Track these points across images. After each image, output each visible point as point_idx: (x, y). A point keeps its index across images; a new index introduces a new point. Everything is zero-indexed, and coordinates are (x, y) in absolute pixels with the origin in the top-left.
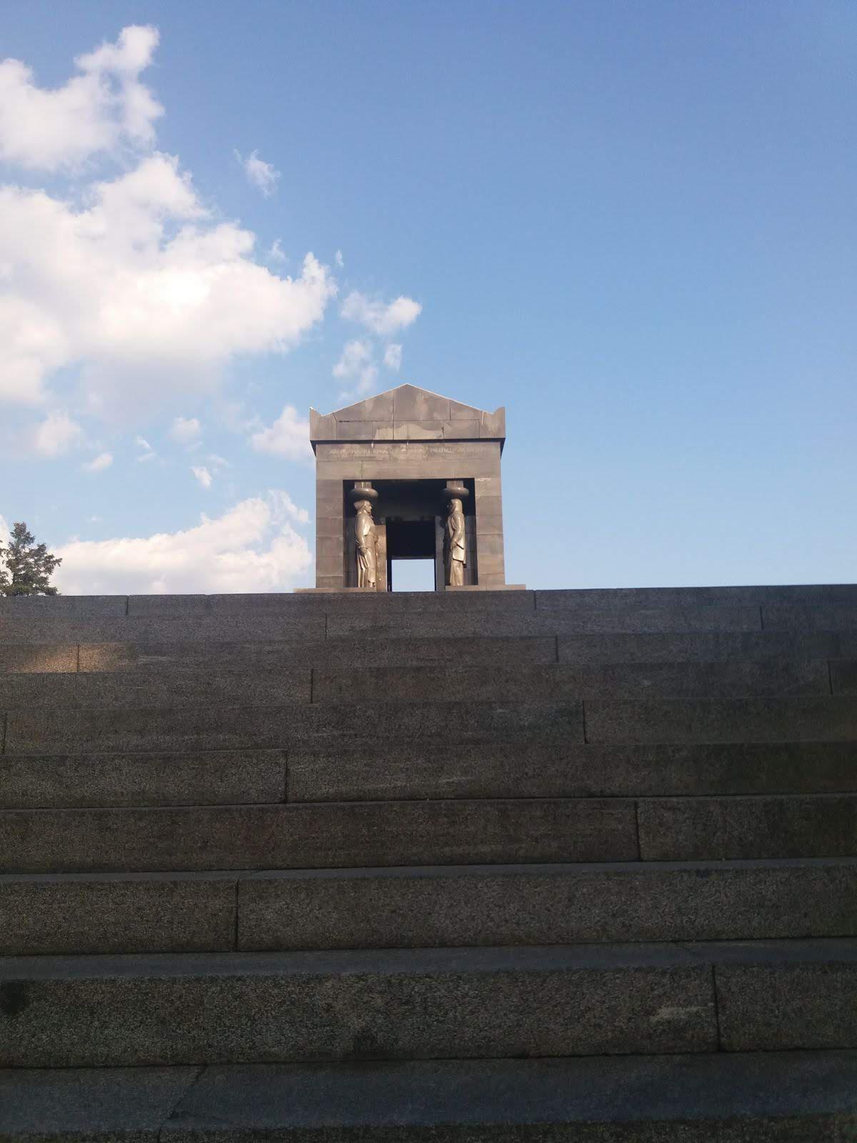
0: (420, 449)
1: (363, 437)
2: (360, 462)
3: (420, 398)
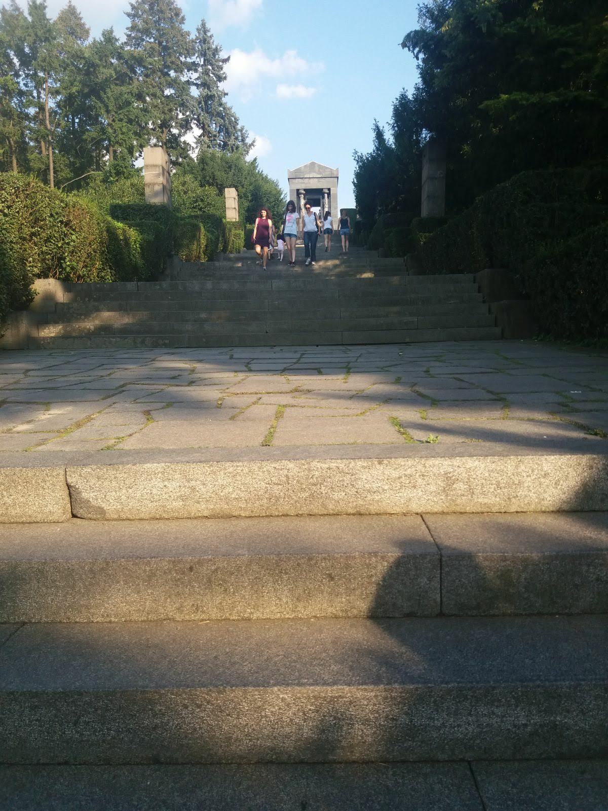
1: (302, 177)
3: (316, 165)
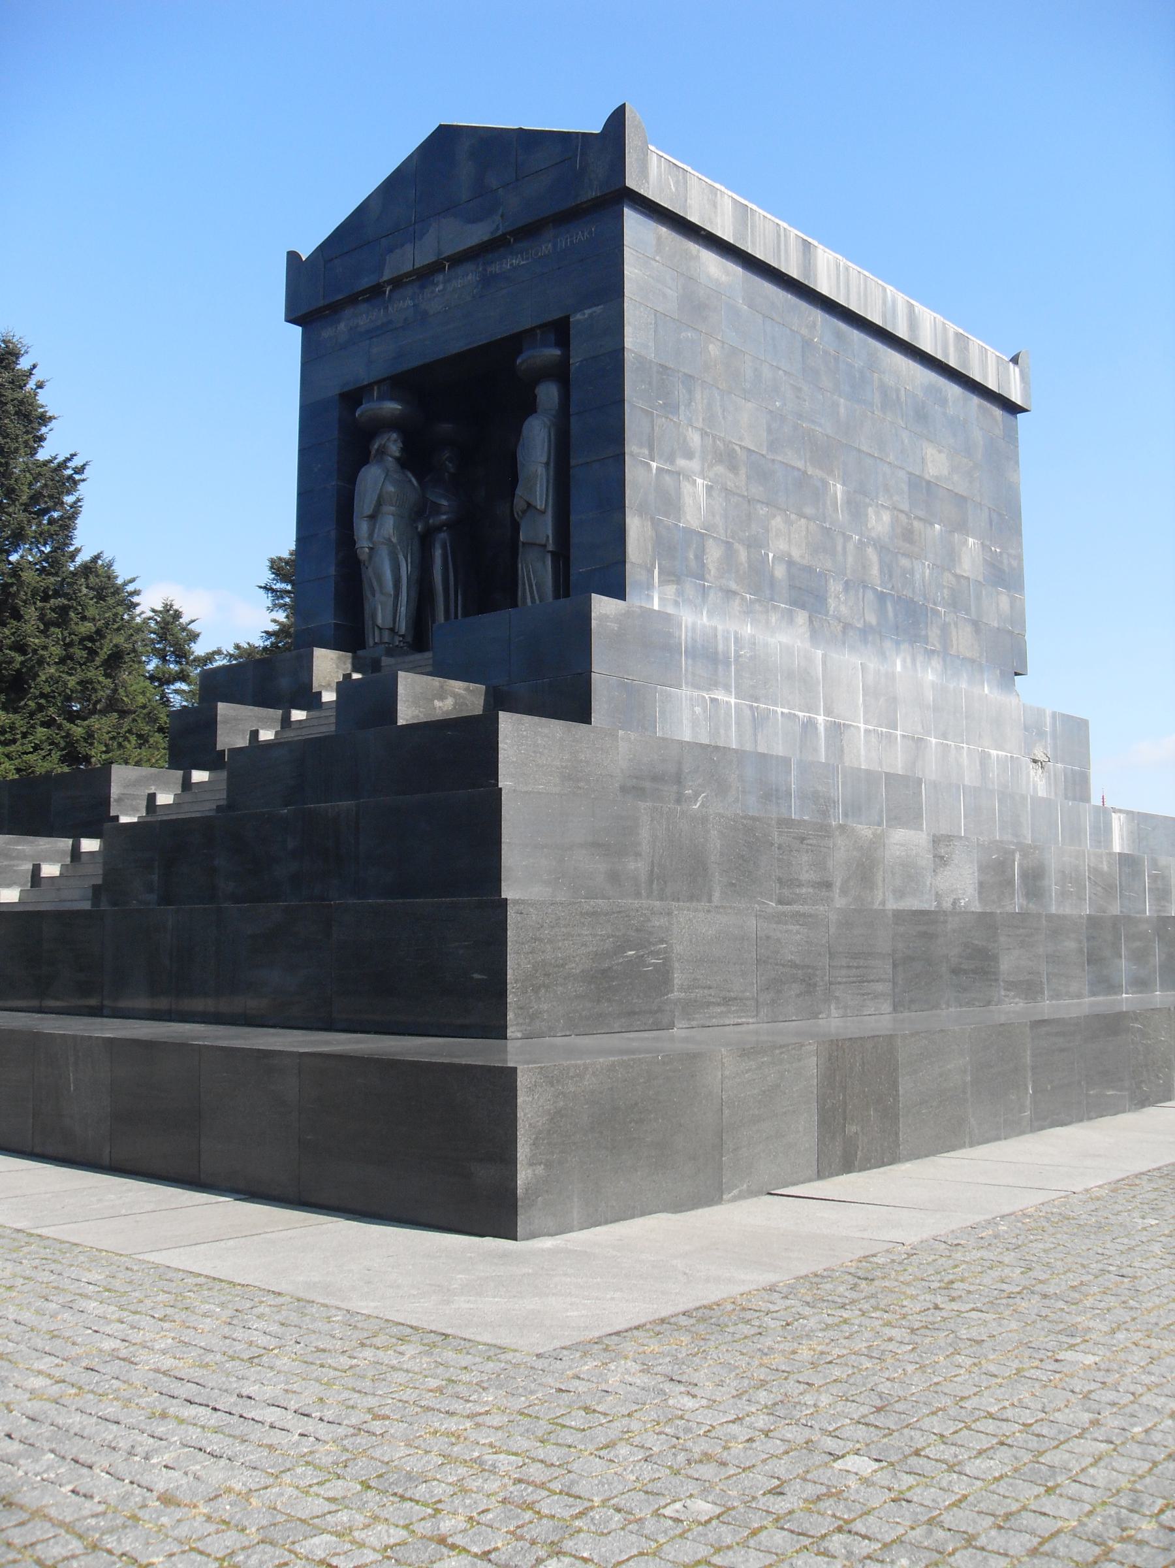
0: (467, 278)
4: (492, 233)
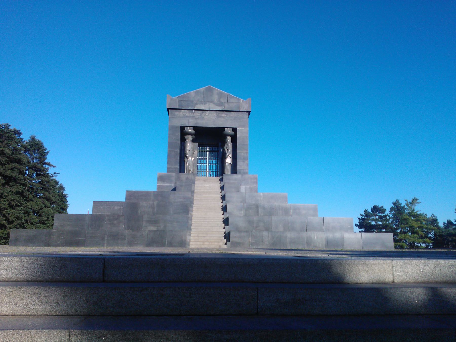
1: (190, 108)
2: (188, 118)
4: (222, 109)
